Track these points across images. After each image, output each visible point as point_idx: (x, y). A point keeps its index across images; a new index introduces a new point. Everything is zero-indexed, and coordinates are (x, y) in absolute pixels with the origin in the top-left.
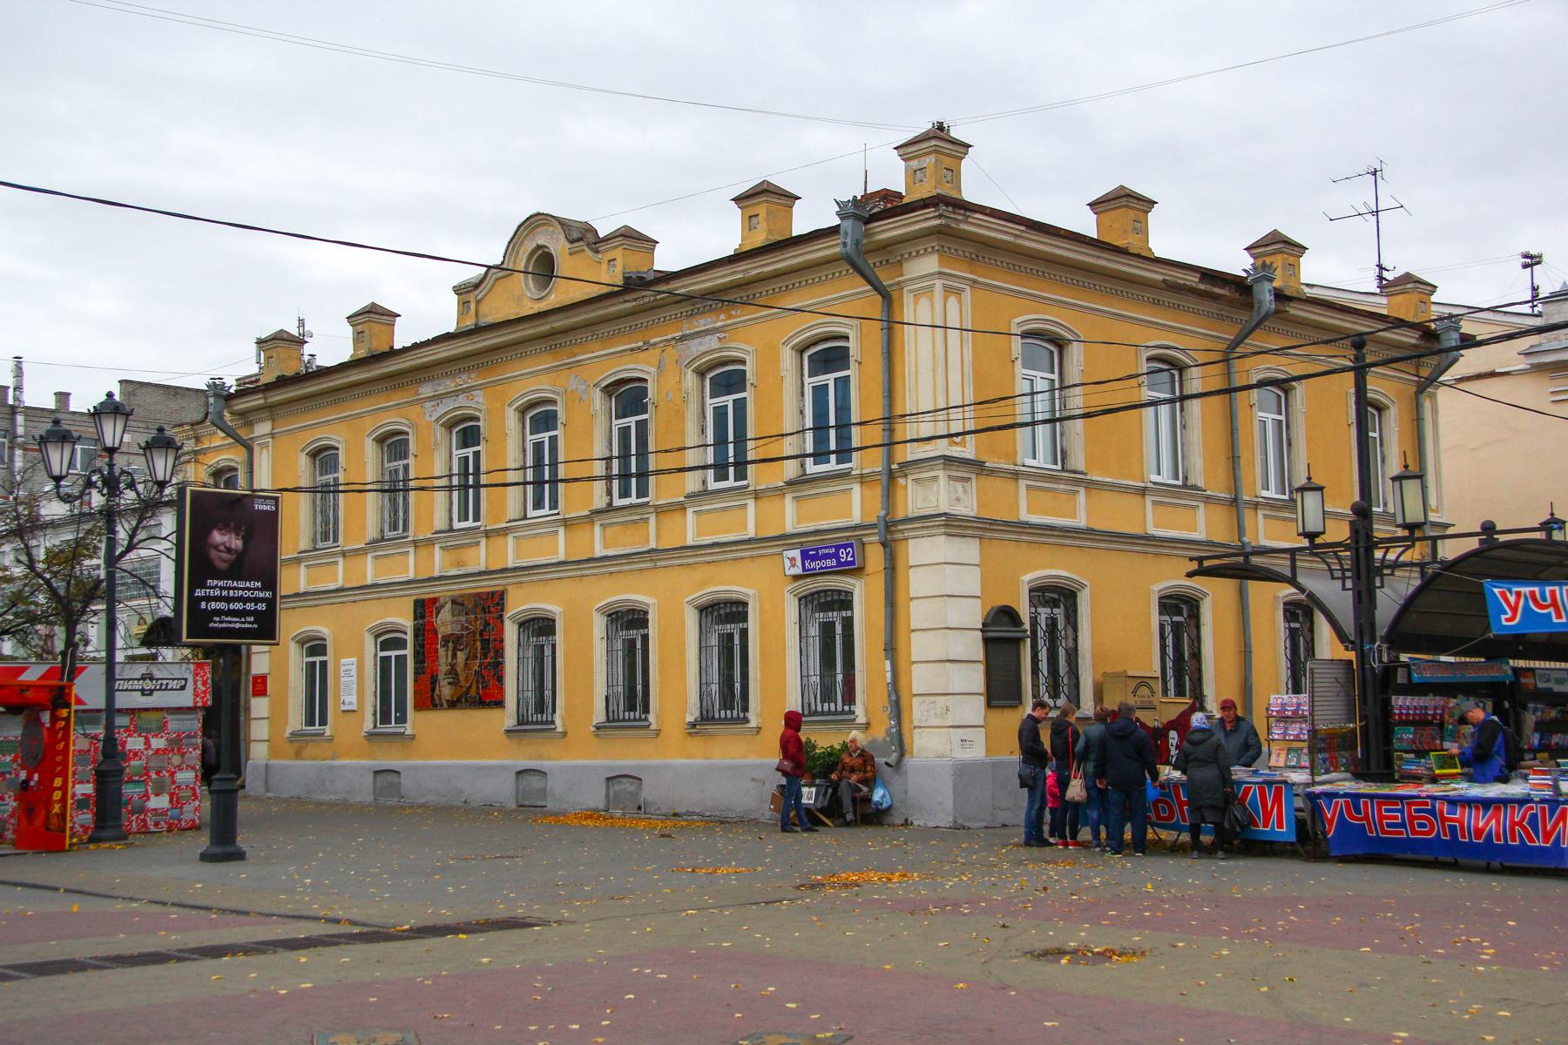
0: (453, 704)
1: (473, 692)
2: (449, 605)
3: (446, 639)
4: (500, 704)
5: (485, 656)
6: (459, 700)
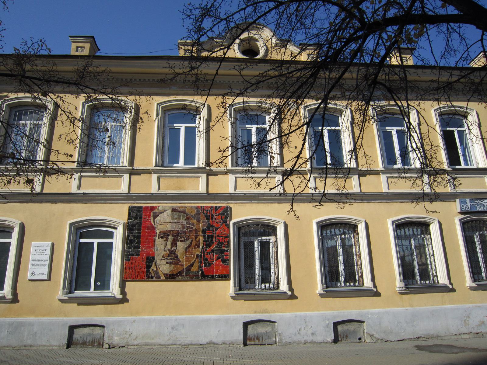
0: (171, 277)
1: (195, 268)
2: (169, 212)
3: (165, 235)
4: (225, 277)
5: (209, 246)
6: (179, 274)
